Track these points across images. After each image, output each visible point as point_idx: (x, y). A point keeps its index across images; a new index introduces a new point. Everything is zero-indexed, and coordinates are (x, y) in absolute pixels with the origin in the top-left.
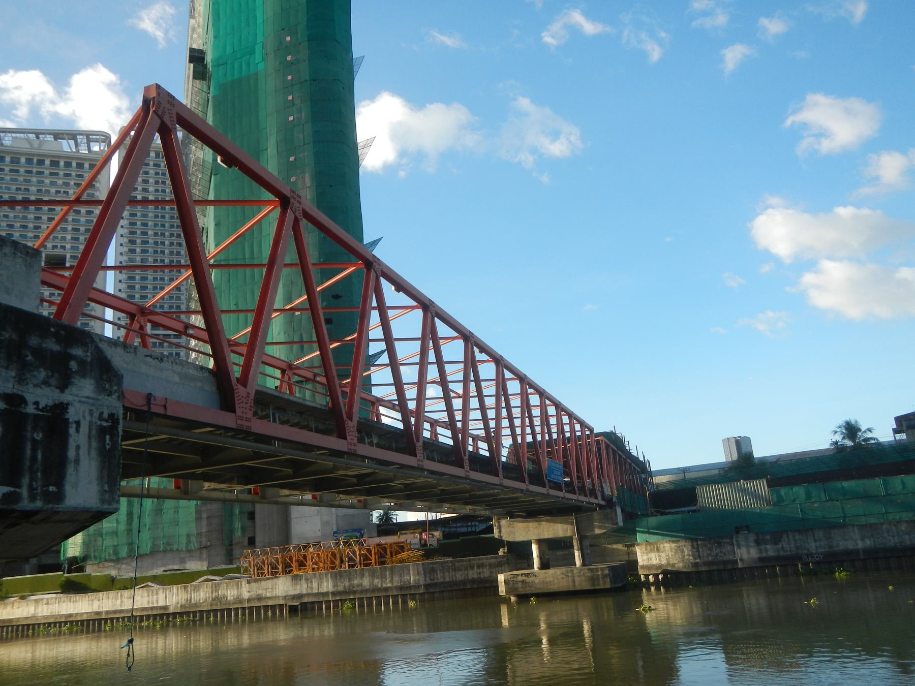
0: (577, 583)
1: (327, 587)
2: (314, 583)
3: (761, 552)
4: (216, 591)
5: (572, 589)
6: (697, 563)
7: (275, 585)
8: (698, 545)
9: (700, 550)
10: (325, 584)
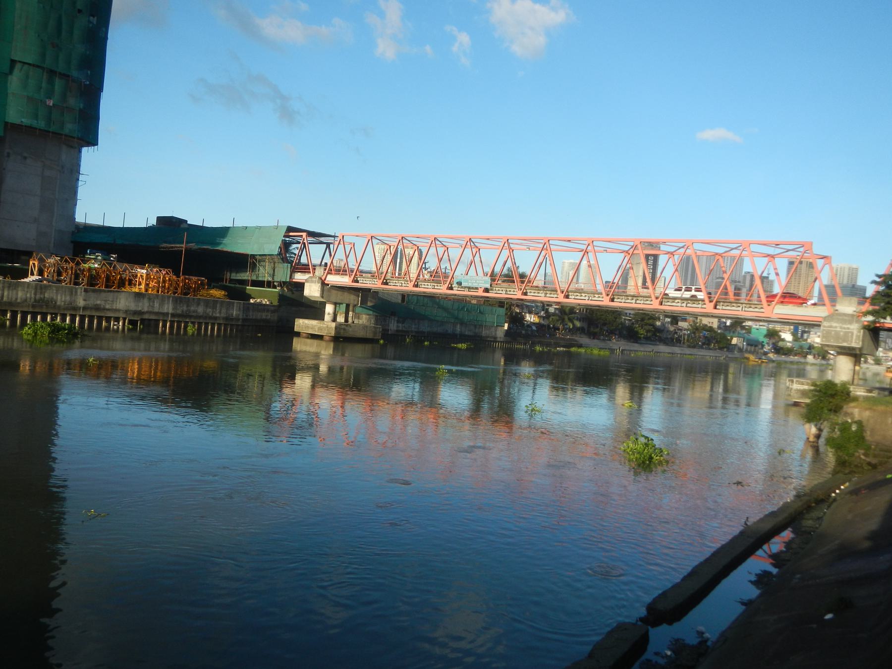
0: (367, 334)
1: (168, 309)
2: (155, 303)
3: (398, 327)
4: (41, 293)
5: (365, 337)
7: (117, 299)
10: (166, 306)
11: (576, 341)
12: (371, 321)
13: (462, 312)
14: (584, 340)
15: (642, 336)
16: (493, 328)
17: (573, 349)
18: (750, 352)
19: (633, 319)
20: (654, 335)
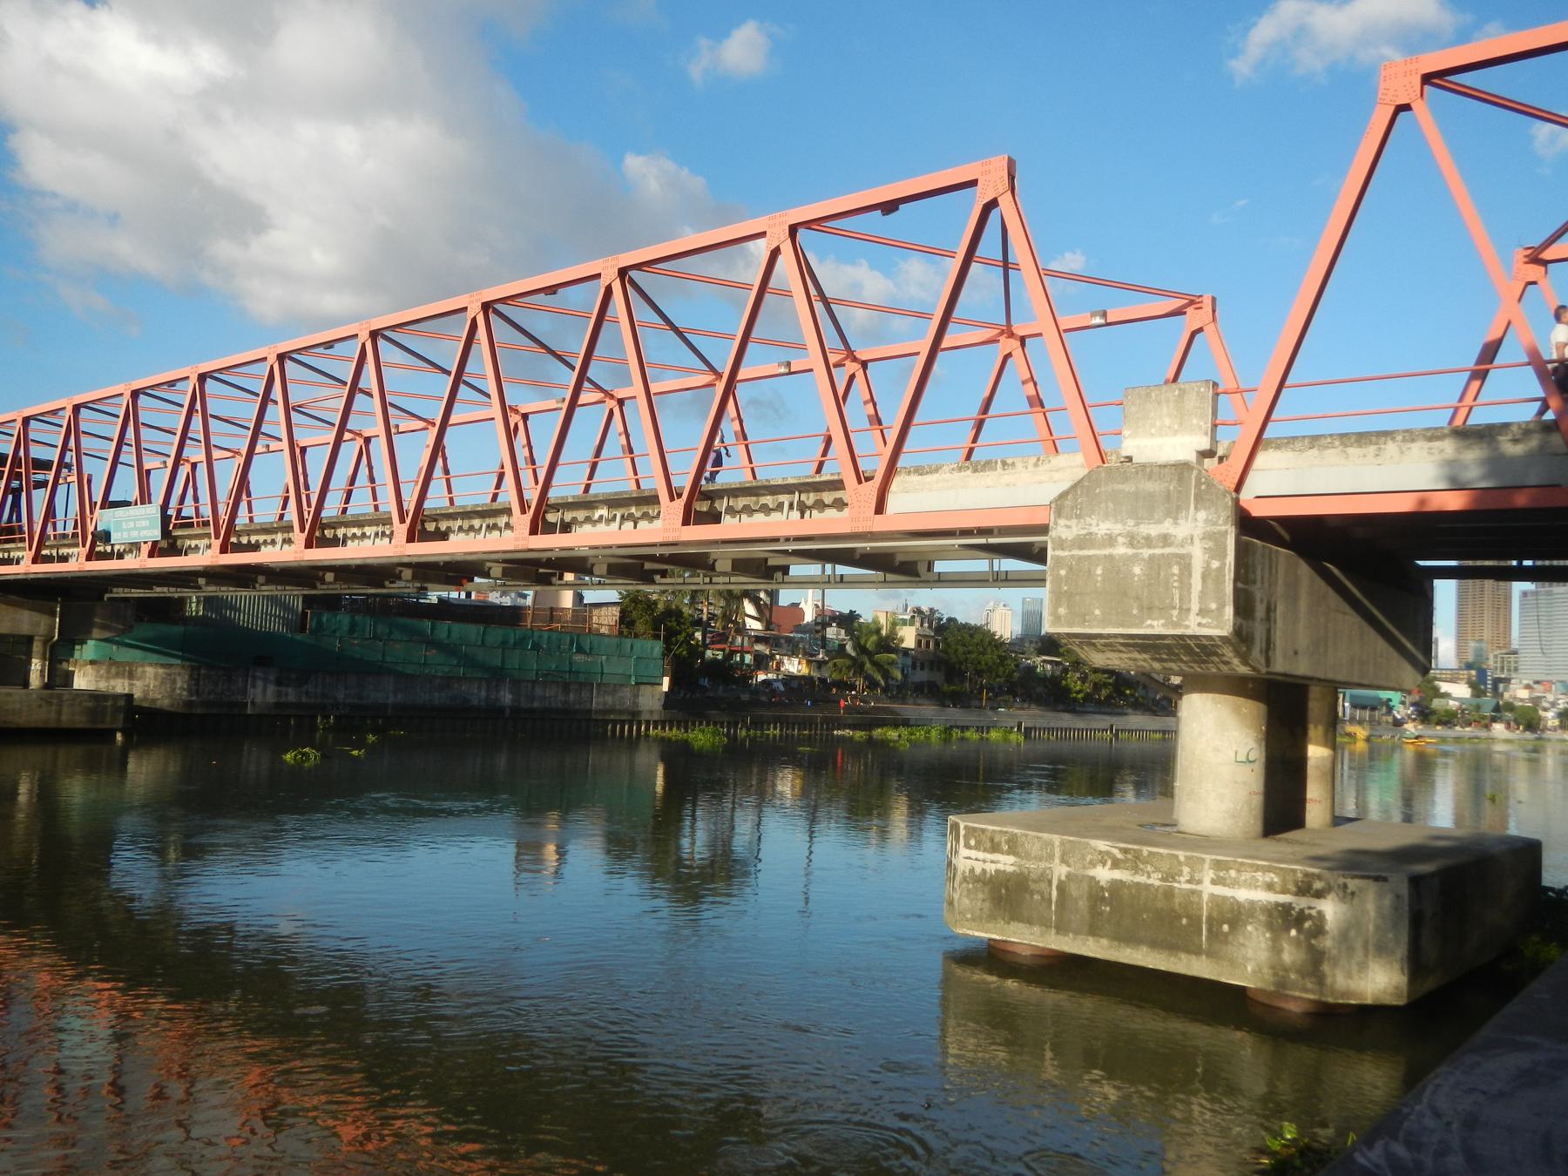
6: (192, 701)
8: (199, 675)
9: (201, 683)
11: (892, 712)
12: (174, 682)
13: (517, 651)
14: (927, 710)
15: (1080, 696)
16: (628, 689)
17: (878, 733)
18: (1360, 722)
19: (1066, 661)
20: (1121, 694)
